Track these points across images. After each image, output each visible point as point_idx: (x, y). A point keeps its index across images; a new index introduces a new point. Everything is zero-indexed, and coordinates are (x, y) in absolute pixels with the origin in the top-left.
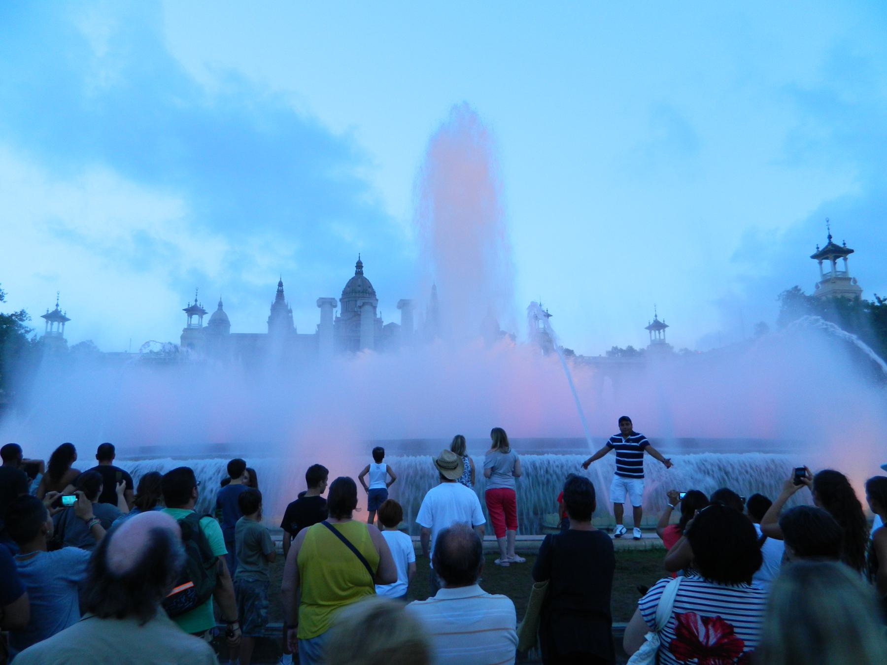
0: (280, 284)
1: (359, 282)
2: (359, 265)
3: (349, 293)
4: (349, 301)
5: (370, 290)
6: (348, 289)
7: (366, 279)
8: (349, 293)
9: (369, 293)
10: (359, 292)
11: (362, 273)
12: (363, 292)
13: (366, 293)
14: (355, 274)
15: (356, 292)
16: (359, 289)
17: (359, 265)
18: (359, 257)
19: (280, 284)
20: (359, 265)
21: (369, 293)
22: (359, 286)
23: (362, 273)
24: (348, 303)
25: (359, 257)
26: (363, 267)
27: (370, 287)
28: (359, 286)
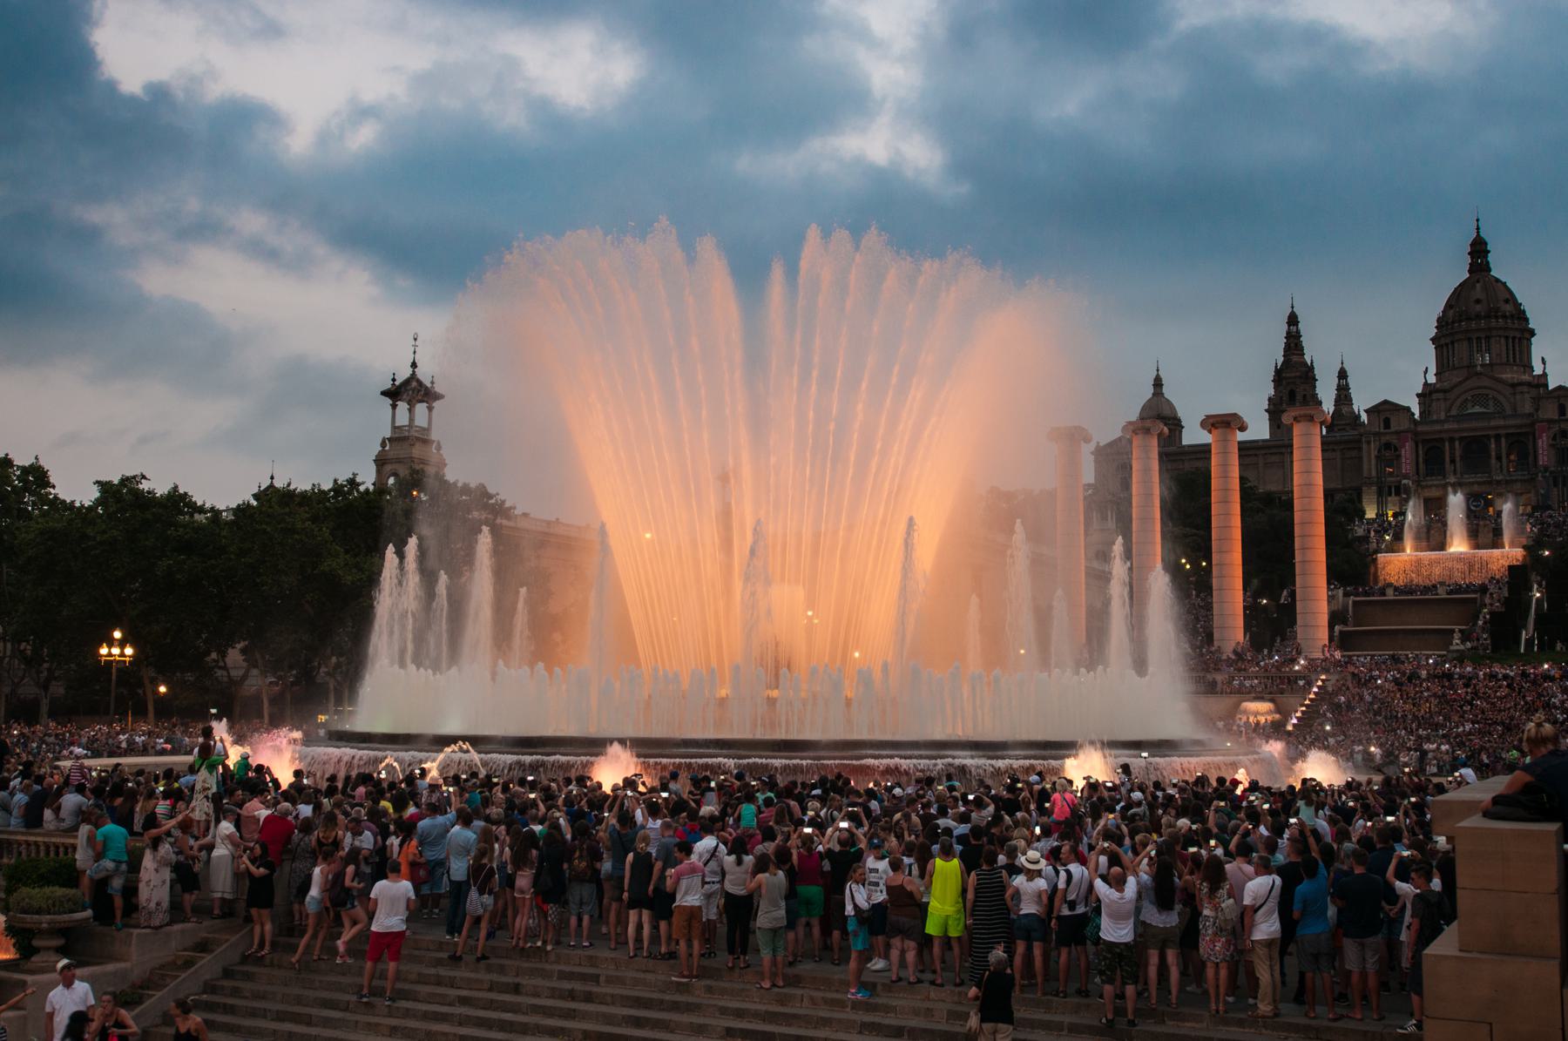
0: (1293, 320)
1: (1478, 292)
2: (1479, 249)
3: (1453, 322)
4: (1453, 343)
5: (1509, 308)
6: (1451, 313)
7: (1497, 280)
8: (1453, 322)
9: (1504, 317)
10: (1478, 317)
11: (1489, 270)
12: (1488, 317)
13: (1497, 317)
14: (1470, 271)
15: (1469, 319)
17: (1479, 249)
18: (1478, 229)
19: (1293, 320)
20: (1478, 248)
21: (1504, 317)
23: (1487, 268)
25: (1478, 229)
26: (1489, 252)
27: (1507, 301)
28: (1478, 301)
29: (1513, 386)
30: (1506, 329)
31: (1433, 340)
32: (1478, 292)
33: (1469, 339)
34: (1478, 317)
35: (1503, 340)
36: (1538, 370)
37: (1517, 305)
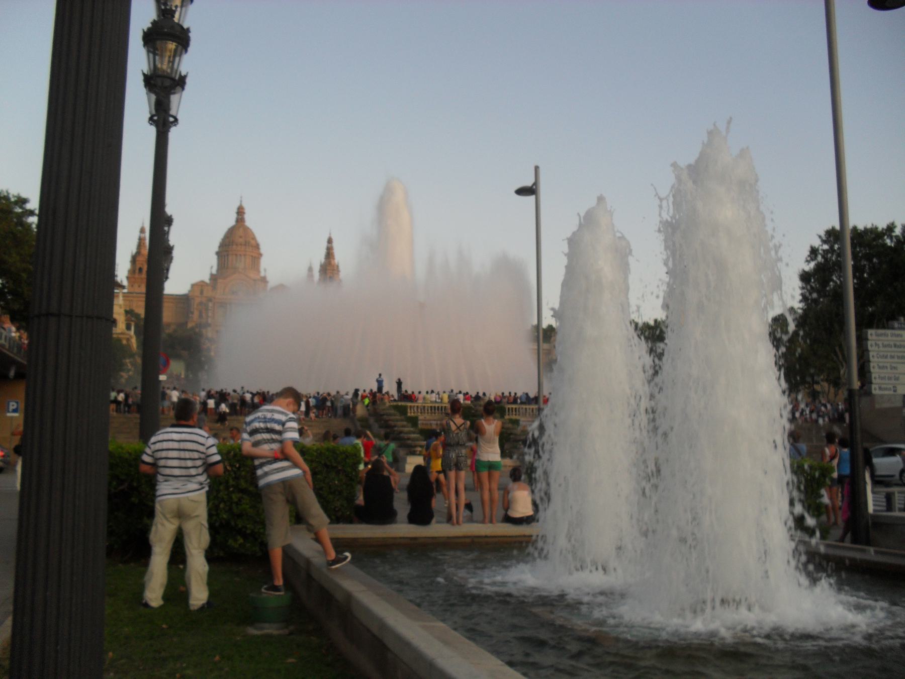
2: (240, 212)
4: (228, 255)
5: (253, 242)
8: (229, 245)
9: (252, 246)
10: (241, 245)
16: (241, 240)
17: (240, 212)
22: (241, 237)
24: (226, 258)
28: (241, 237)
29: (255, 280)
30: (252, 252)
31: (217, 253)
32: (240, 232)
33: (236, 255)
34: (241, 245)
35: (251, 257)
36: (262, 274)
37: (256, 241)
